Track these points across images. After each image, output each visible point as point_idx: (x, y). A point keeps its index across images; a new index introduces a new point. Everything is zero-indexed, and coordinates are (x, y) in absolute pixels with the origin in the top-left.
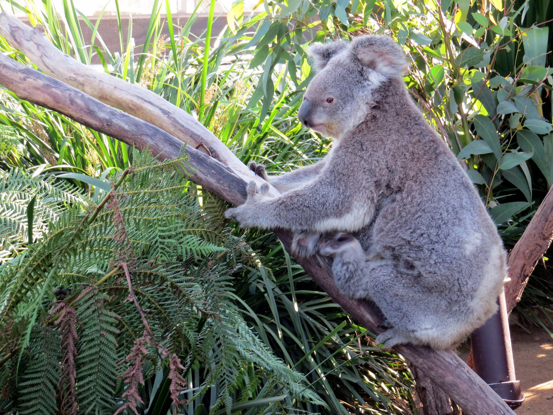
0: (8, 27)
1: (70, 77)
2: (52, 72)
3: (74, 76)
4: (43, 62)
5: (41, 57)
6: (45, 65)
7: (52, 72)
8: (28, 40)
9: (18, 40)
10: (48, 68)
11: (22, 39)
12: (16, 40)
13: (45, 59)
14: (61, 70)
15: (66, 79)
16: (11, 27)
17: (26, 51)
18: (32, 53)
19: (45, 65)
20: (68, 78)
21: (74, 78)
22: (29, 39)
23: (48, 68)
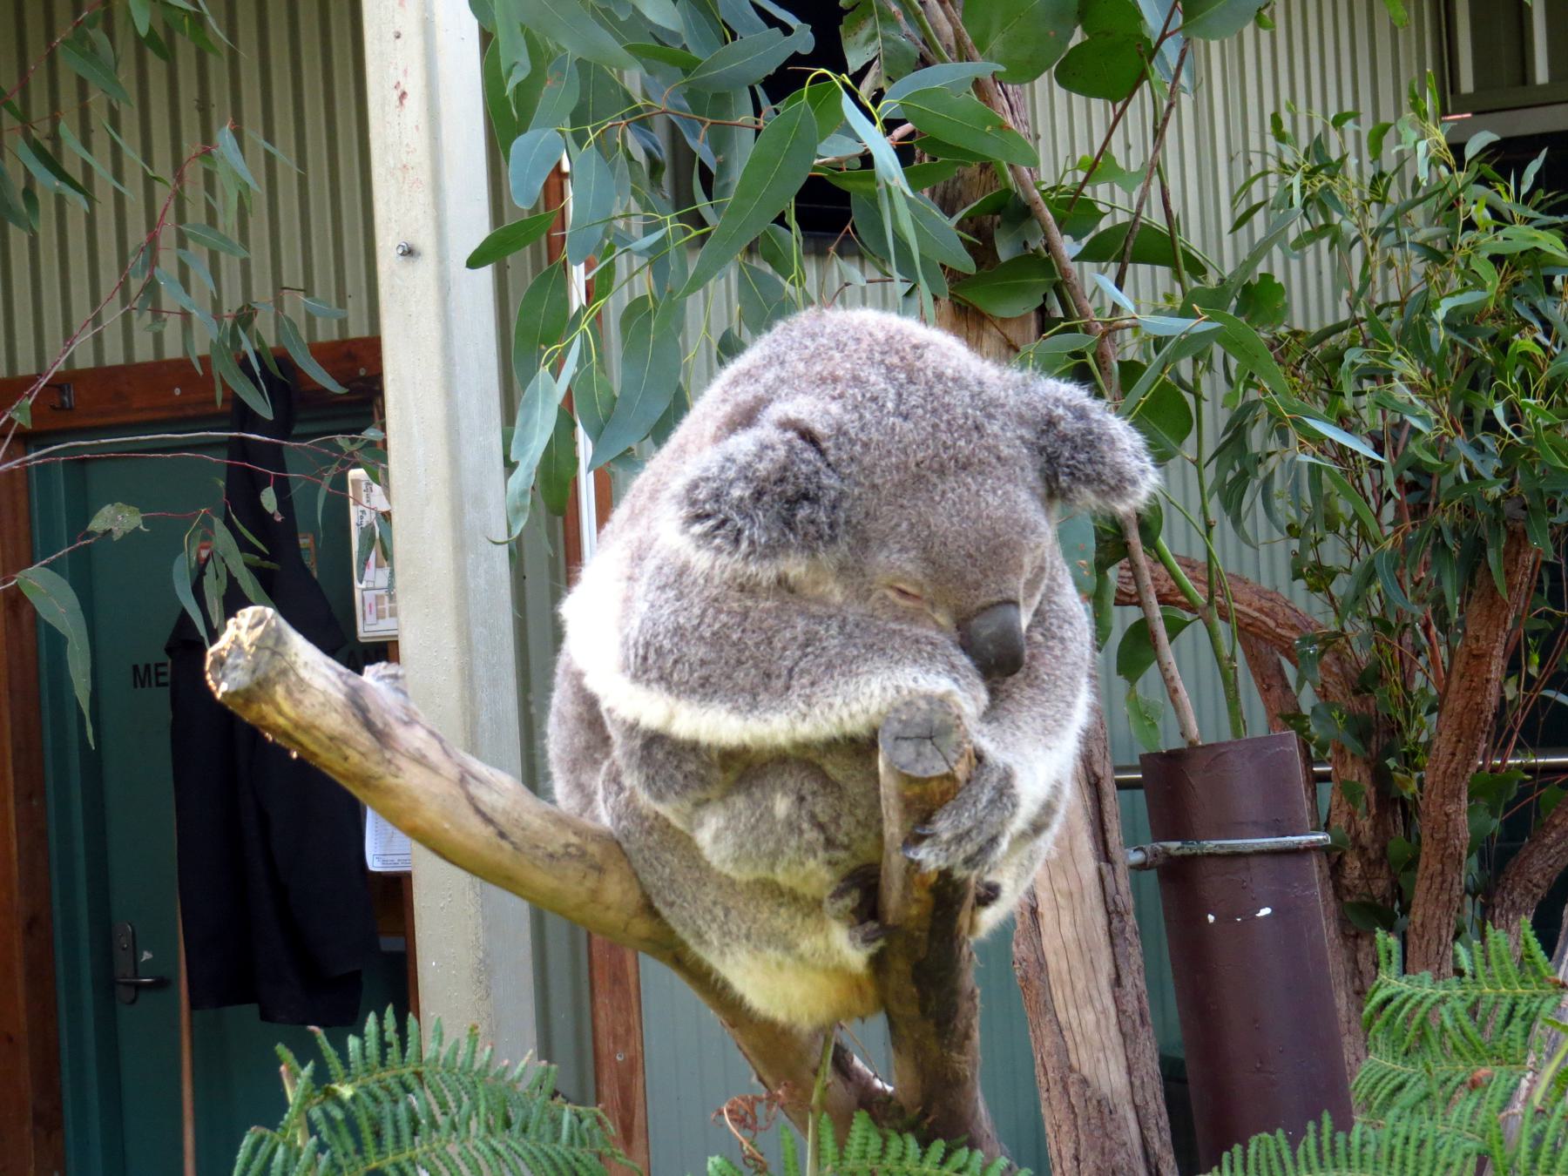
0: (330, 673)
1: (567, 845)
2: (502, 835)
3: (574, 839)
4: (471, 800)
5: (462, 781)
6: (478, 811)
7: (502, 835)
8: (406, 724)
9: (380, 725)
10: (488, 820)
11: (391, 720)
12: (368, 725)
13: (473, 788)
14: (537, 823)
15: (551, 856)
16: (340, 675)
17: (403, 762)
18: (434, 769)
19: (478, 811)
20: (561, 851)
21: (578, 848)
22: (406, 719)
23: (488, 820)
